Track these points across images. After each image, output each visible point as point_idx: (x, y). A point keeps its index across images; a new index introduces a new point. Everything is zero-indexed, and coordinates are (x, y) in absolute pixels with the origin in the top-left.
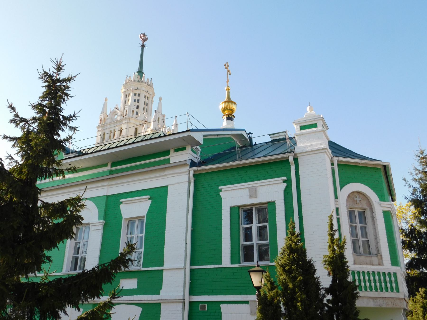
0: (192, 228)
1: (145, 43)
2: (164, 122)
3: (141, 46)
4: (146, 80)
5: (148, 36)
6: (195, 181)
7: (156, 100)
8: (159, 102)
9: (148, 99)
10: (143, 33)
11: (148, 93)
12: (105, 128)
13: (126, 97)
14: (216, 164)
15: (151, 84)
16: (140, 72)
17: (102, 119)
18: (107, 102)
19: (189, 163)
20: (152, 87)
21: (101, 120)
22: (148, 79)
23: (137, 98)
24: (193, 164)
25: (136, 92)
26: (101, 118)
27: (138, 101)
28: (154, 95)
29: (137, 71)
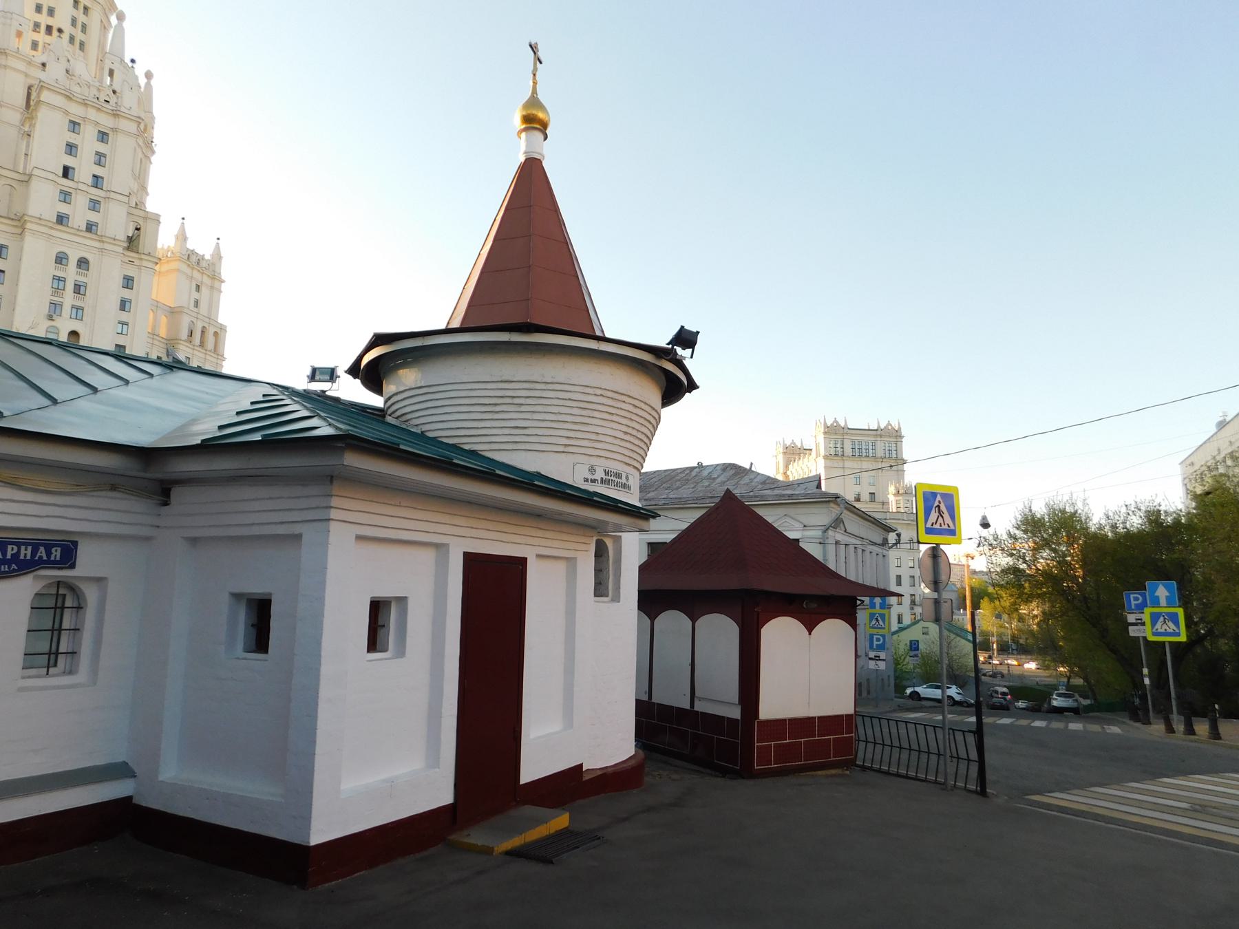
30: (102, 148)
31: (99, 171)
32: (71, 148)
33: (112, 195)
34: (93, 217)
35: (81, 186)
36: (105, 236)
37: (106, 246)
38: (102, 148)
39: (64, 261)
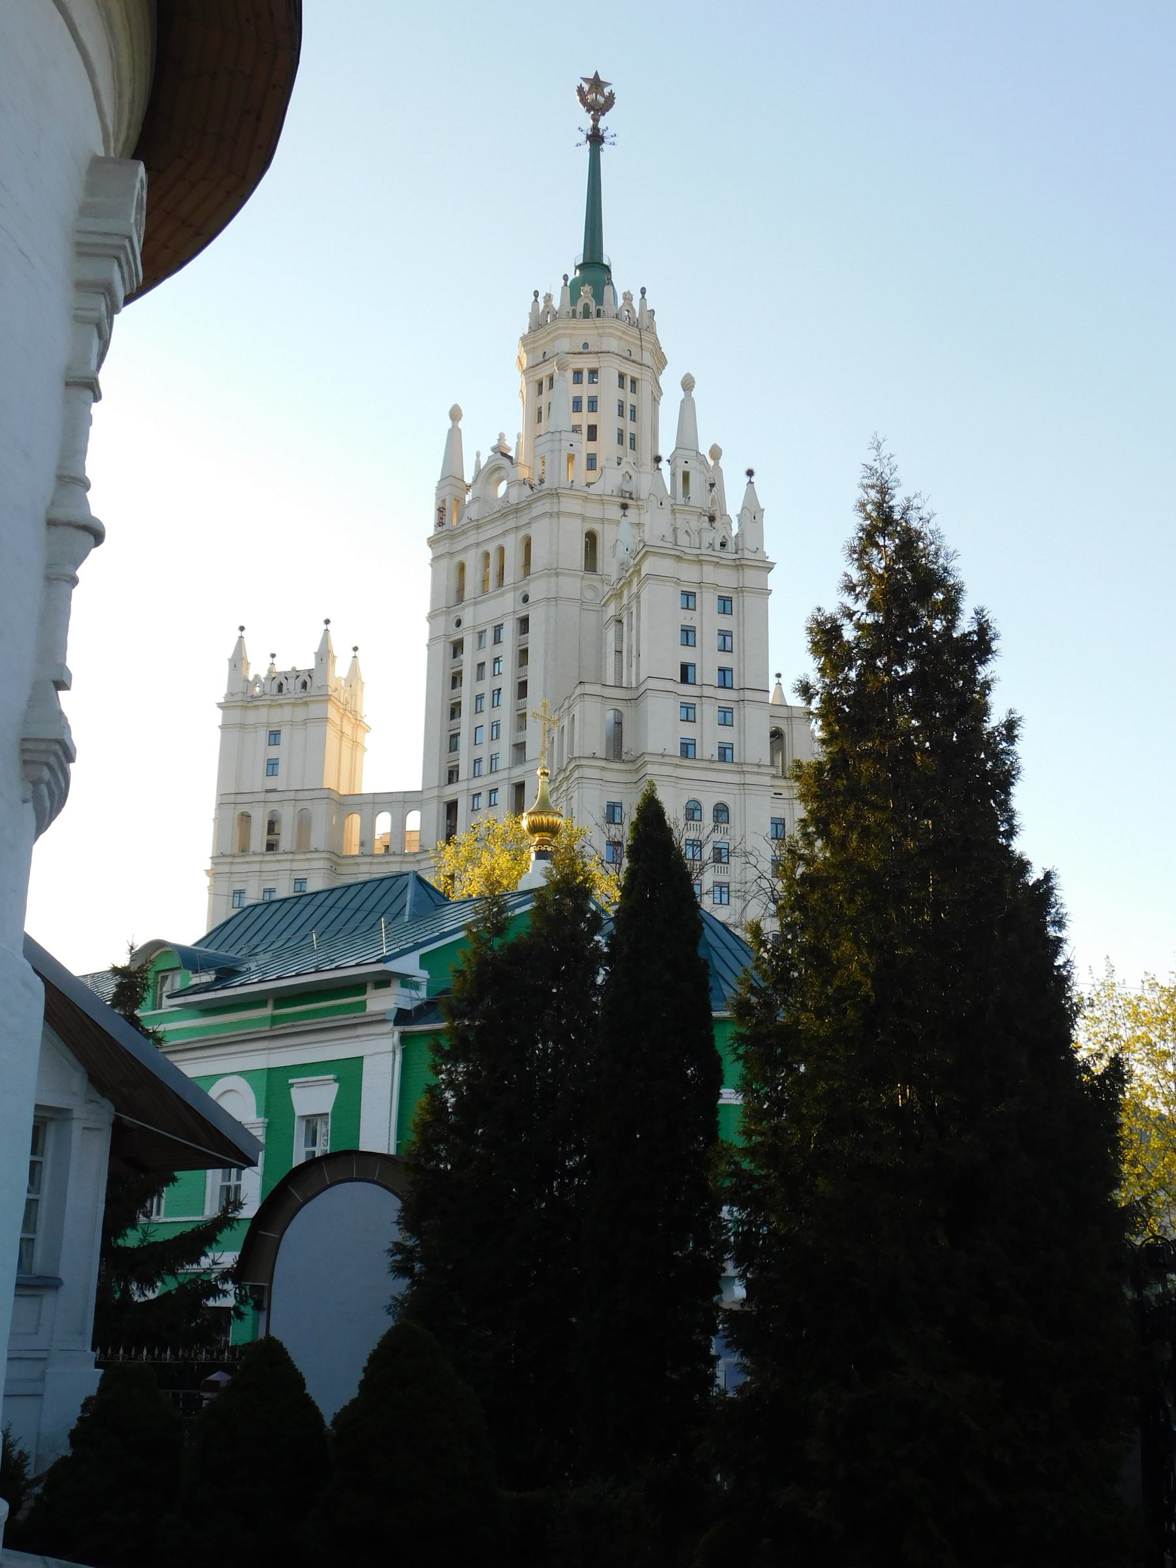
0: (398, 1140)
1: (601, 125)
2: (712, 485)
3: (589, 137)
4: (620, 302)
5: (616, 84)
6: (404, 1052)
7: (670, 381)
8: (682, 401)
9: (633, 390)
10: (592, 77)
11: (634, 362)
12: (460, 546)
13: (540, 392)
14: (430, 1023)
15: (646, 315)
17: (447, 506)
18: (461, 425)
19: (392, 1016)
20: (651, 329)
21: (441, 511)
22: (628, 297)
23: (585, 390)
24: (402, 1017)
25: (578, 366)
26: (444, 501)
27: (593, 405)
28: (661, 362)
29: (580, 261)
30: (726, 623)
31: (726, 660)
32: (688, 635)
33: (749, 695)
34: (727, 735)
35: (708, 691)
36: (745, 763)
37: (749, 779)
38: (726, 623)
39: (697, 815)
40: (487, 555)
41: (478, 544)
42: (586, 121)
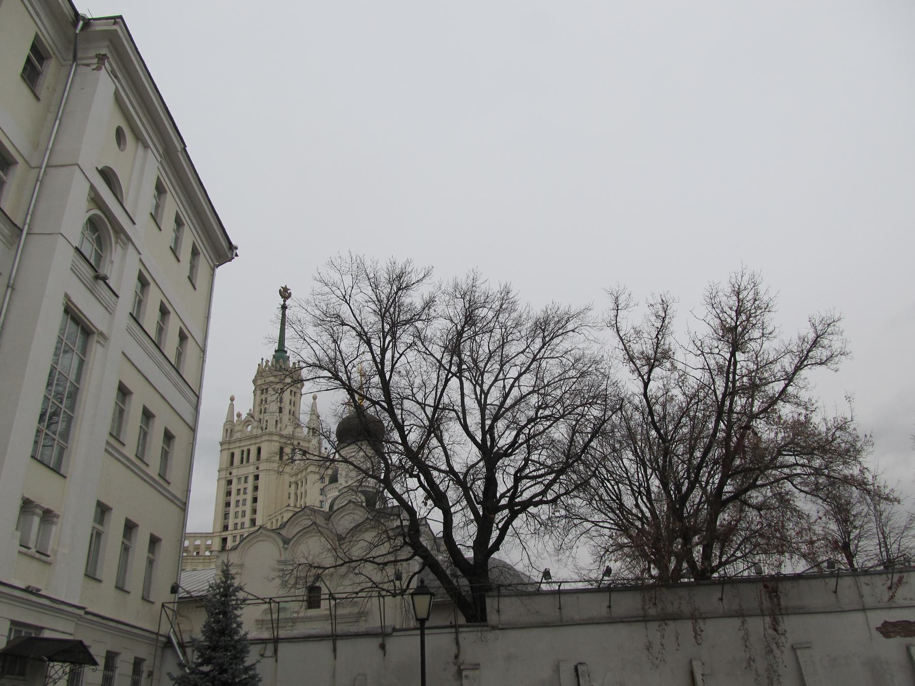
4: (291, 365)
16: (281, 350)
40: (243, 452)
41: (240, 447)
42: (281, 301)
